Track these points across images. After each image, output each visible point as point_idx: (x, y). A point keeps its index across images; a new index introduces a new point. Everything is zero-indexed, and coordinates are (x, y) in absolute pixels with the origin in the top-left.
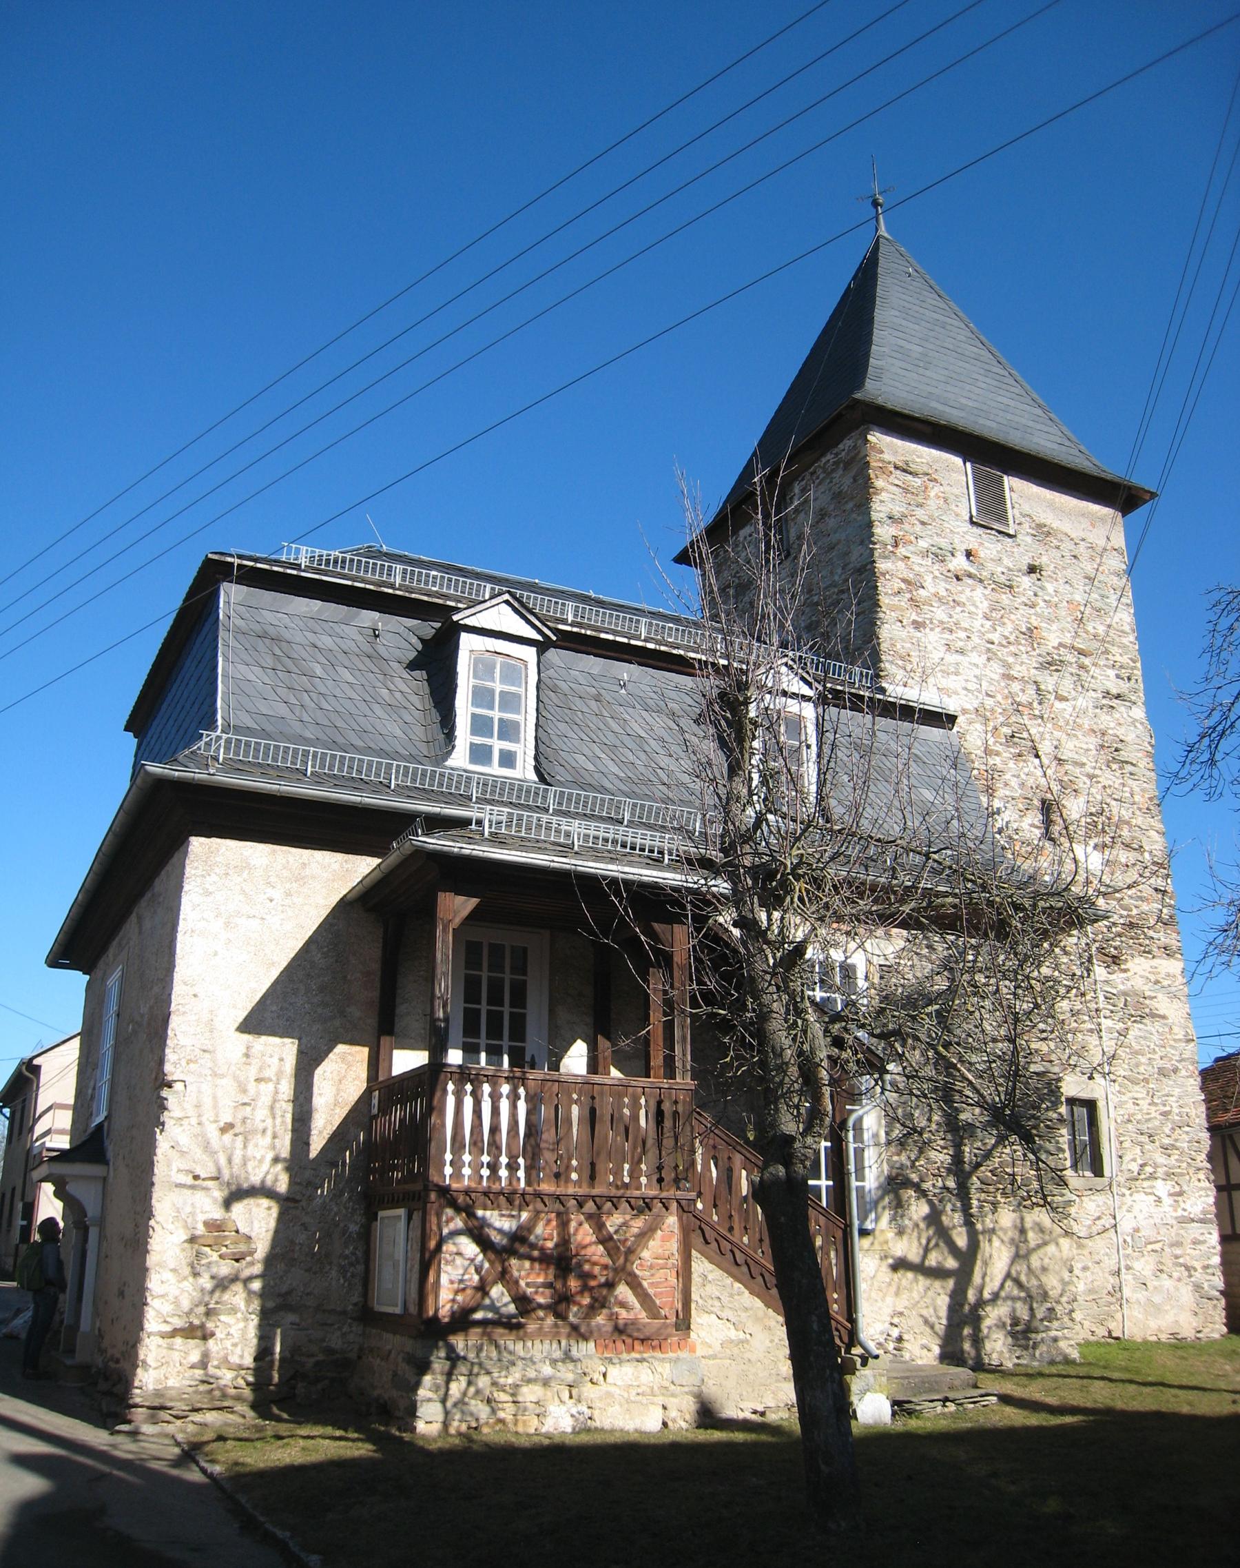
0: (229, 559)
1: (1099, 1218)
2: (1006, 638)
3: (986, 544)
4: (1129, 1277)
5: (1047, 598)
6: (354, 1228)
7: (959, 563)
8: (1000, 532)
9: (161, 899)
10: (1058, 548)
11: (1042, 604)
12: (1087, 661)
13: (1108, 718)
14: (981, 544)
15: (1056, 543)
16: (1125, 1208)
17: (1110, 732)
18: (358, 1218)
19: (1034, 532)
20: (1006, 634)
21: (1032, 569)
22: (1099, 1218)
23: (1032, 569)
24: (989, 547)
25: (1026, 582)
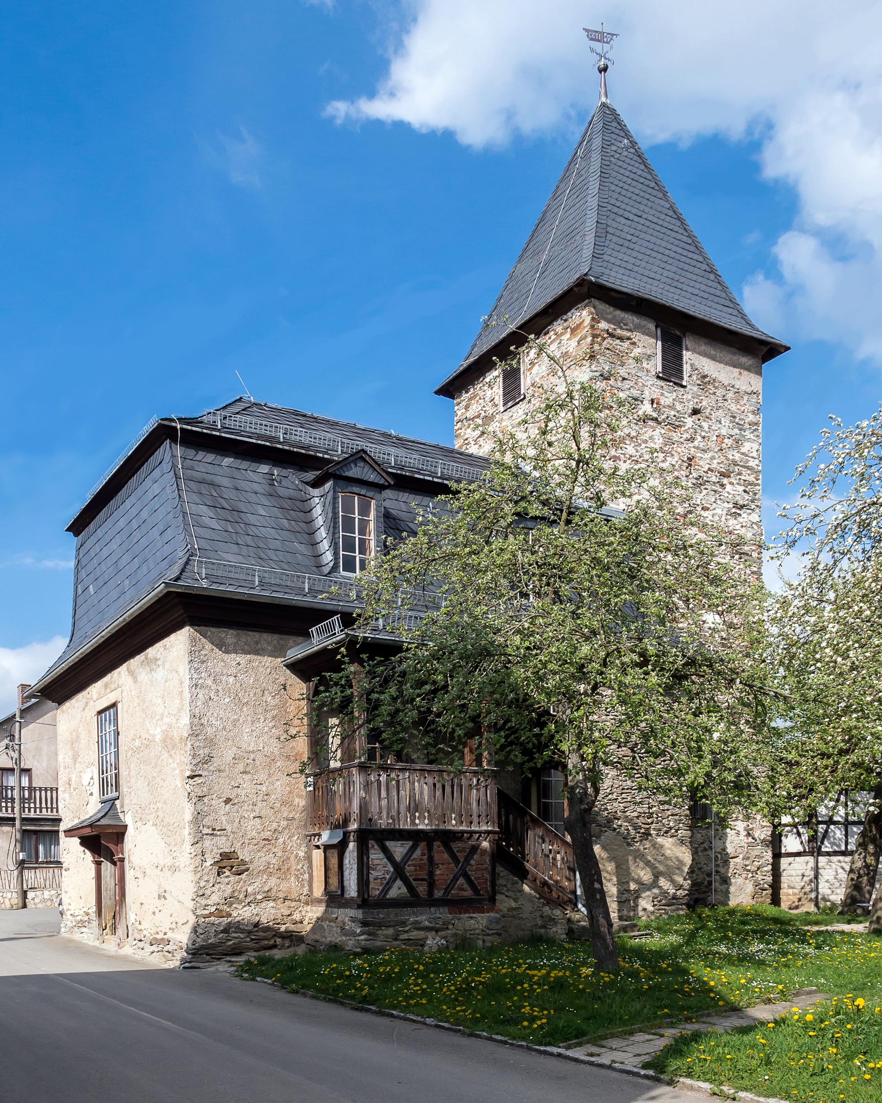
0: (174, 424)
1: (702, 843)
2: (673, 466)
3: (666, 394)
4: (718, 877)
5: (703, 434)
6: (301, 854)
7: (646, 408)
8: (675, 383)
9: (159, 662)
10: (714, 393)
11: (699, 439)
12: (725, 481)
13: (735, 522)
14: (662, 394)
15: (713, 390)
16: (717, 838)
17: (736, 532)
18: (303, 849)
19: (699, 382)
20: (674, 463)
21: (695, 412)
22: (702, 843)
23: (695, 412)
24: (668, 396)
25: (689, 421)
